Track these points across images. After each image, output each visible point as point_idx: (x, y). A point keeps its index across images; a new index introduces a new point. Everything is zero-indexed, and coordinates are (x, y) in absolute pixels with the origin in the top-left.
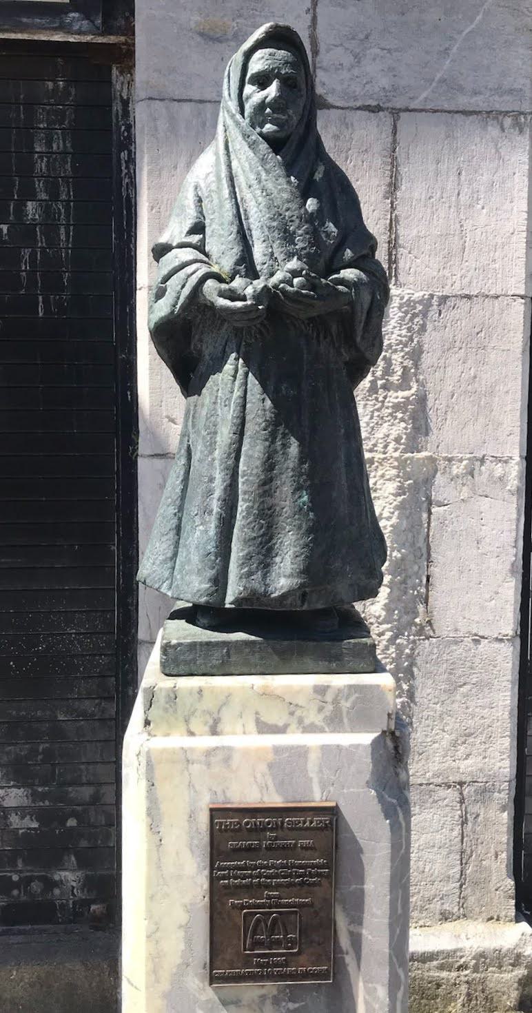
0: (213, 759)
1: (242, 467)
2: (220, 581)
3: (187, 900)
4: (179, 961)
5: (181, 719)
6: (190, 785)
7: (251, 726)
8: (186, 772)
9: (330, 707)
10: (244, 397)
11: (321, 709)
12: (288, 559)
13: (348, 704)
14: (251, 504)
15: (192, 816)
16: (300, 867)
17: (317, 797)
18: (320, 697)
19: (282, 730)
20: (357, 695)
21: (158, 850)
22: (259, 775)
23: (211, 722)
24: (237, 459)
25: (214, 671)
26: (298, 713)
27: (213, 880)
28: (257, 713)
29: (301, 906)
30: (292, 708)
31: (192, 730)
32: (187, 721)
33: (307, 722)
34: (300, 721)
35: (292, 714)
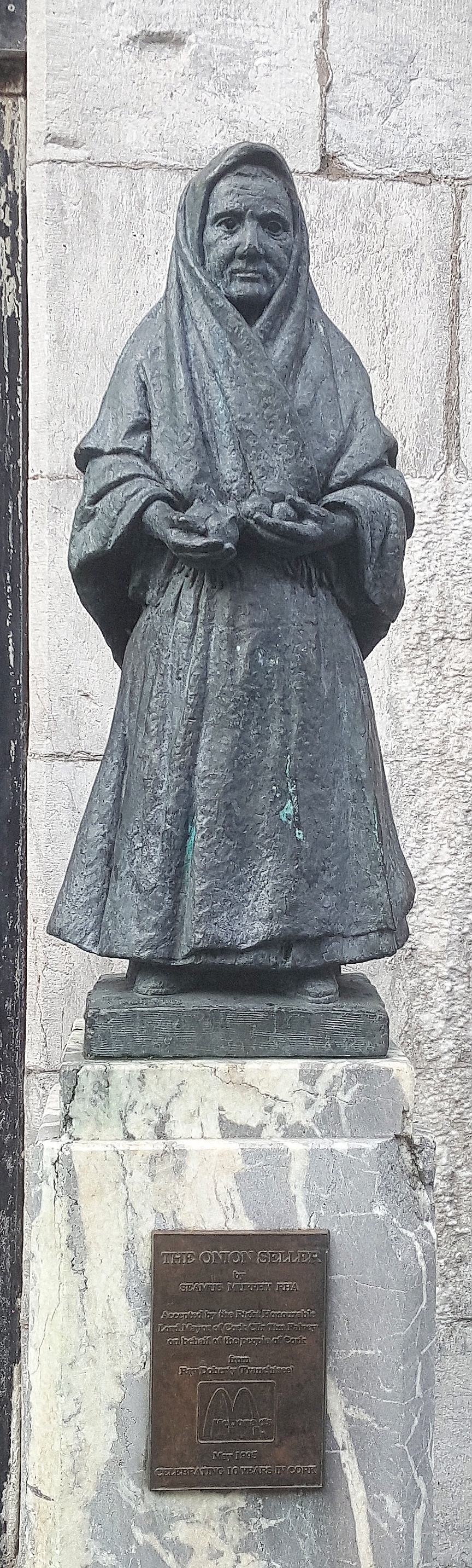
0: (159, 1169)
1: (201, 767)
2: (171, 925)
3: (121, 1369)
4: (108, 1456)
5: (115, 1115)
6: (128, 1204)
7: (213, 1127)
8: (122, 1186)
9: (322, 1101)
10: (205, 668)
11: (309, 1105)
12: (265, 896)
13: (348, 1098)
14: (214, 818)
15: (129, 1249)
16: (277, 1319)
17: (303, 1222)
18: (308, 1087)
19: (255, 1133)
20: (359, 1085)
21: (82, 1297)
22: (222, 1191)
23: (156, 1120)
24: (194, 754)
25: (161, 1051)
26: (278, 1109)
27: (156, 1337)
28: (220, 1109)
29: (280, 1373)
30: (270, 1102)
31: (131, 1132)
32: (123, 1119)
33: (290, 1121)
34: (281, 1120)
35: (269, 1109)
